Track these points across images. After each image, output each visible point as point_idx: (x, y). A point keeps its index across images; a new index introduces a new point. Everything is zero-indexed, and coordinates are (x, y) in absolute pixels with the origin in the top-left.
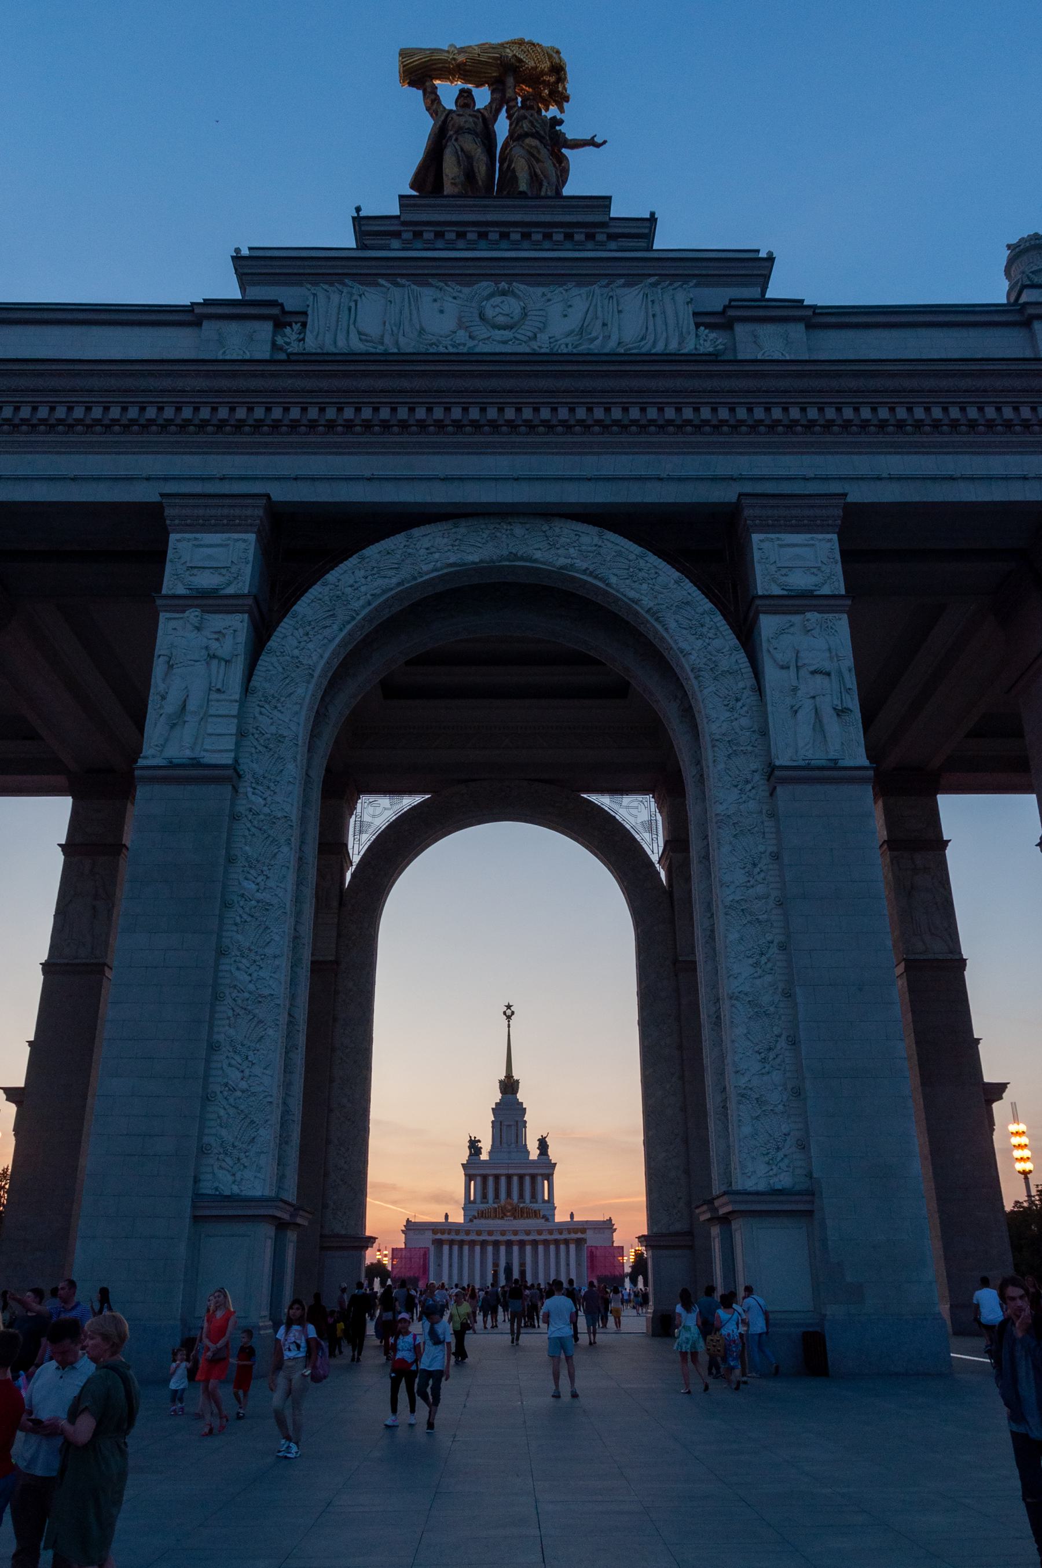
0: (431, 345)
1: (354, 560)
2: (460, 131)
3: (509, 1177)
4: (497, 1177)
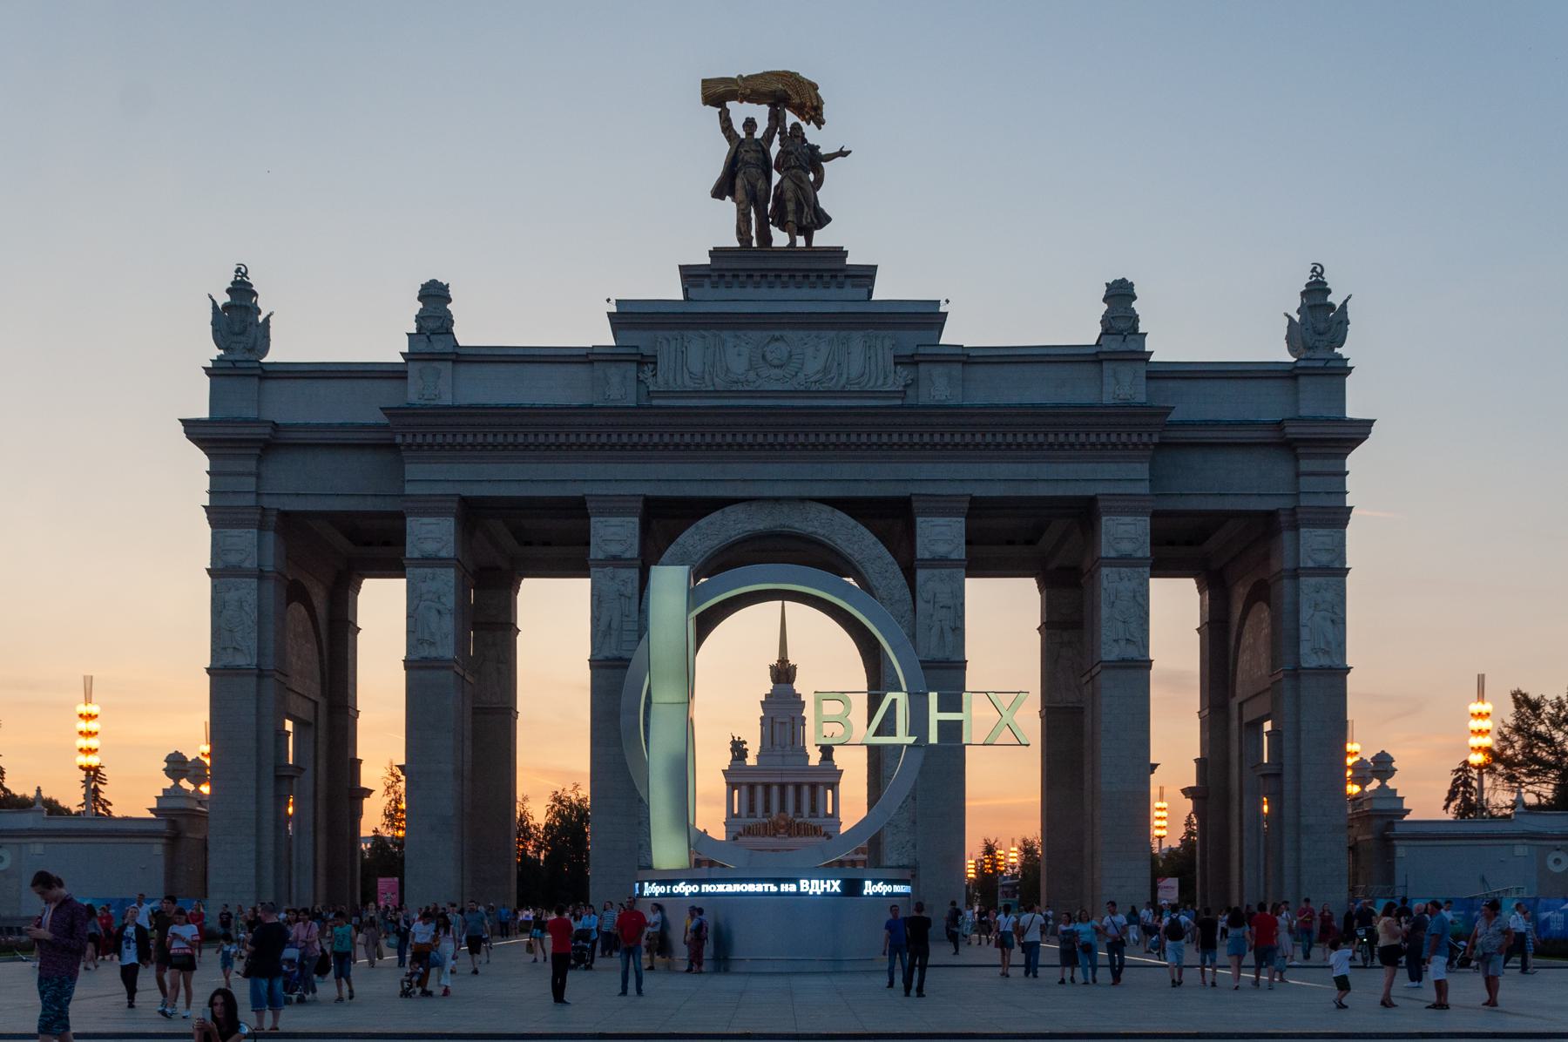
1: (692, 529)
2: (747, 163)
4: (767, 787)
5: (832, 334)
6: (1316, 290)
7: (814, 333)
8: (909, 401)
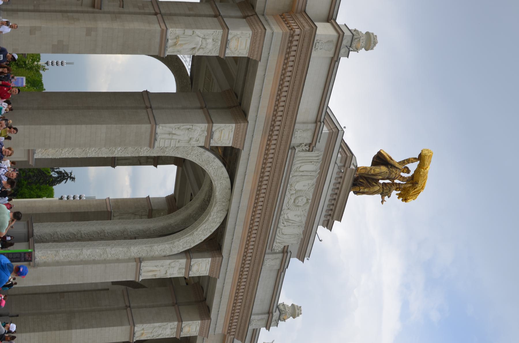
0: (291, 185)
7: (306, 215)
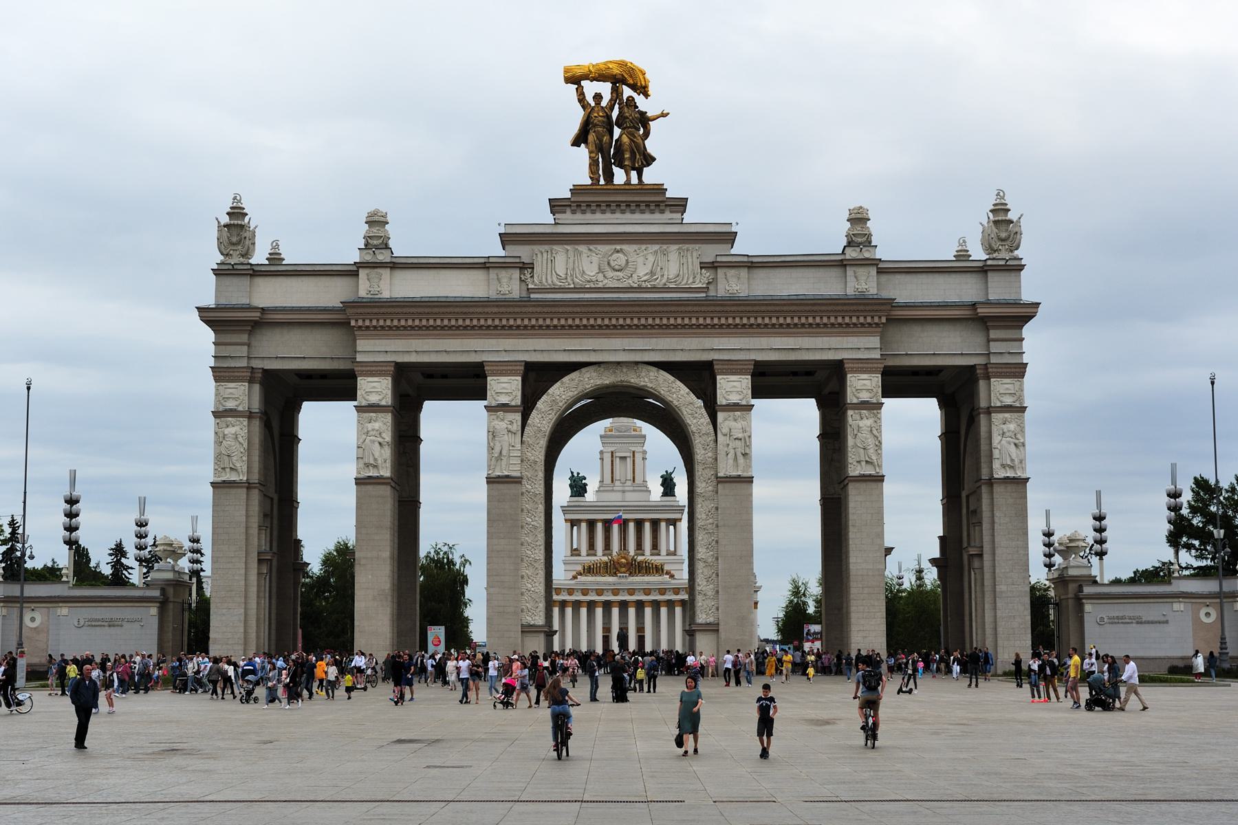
1: (558, 384)
2: (596, 125)
3: (624, 524)
5: (656, 247)
6: (1000, 209)
7: (644, 247)
8: (712, 293)
